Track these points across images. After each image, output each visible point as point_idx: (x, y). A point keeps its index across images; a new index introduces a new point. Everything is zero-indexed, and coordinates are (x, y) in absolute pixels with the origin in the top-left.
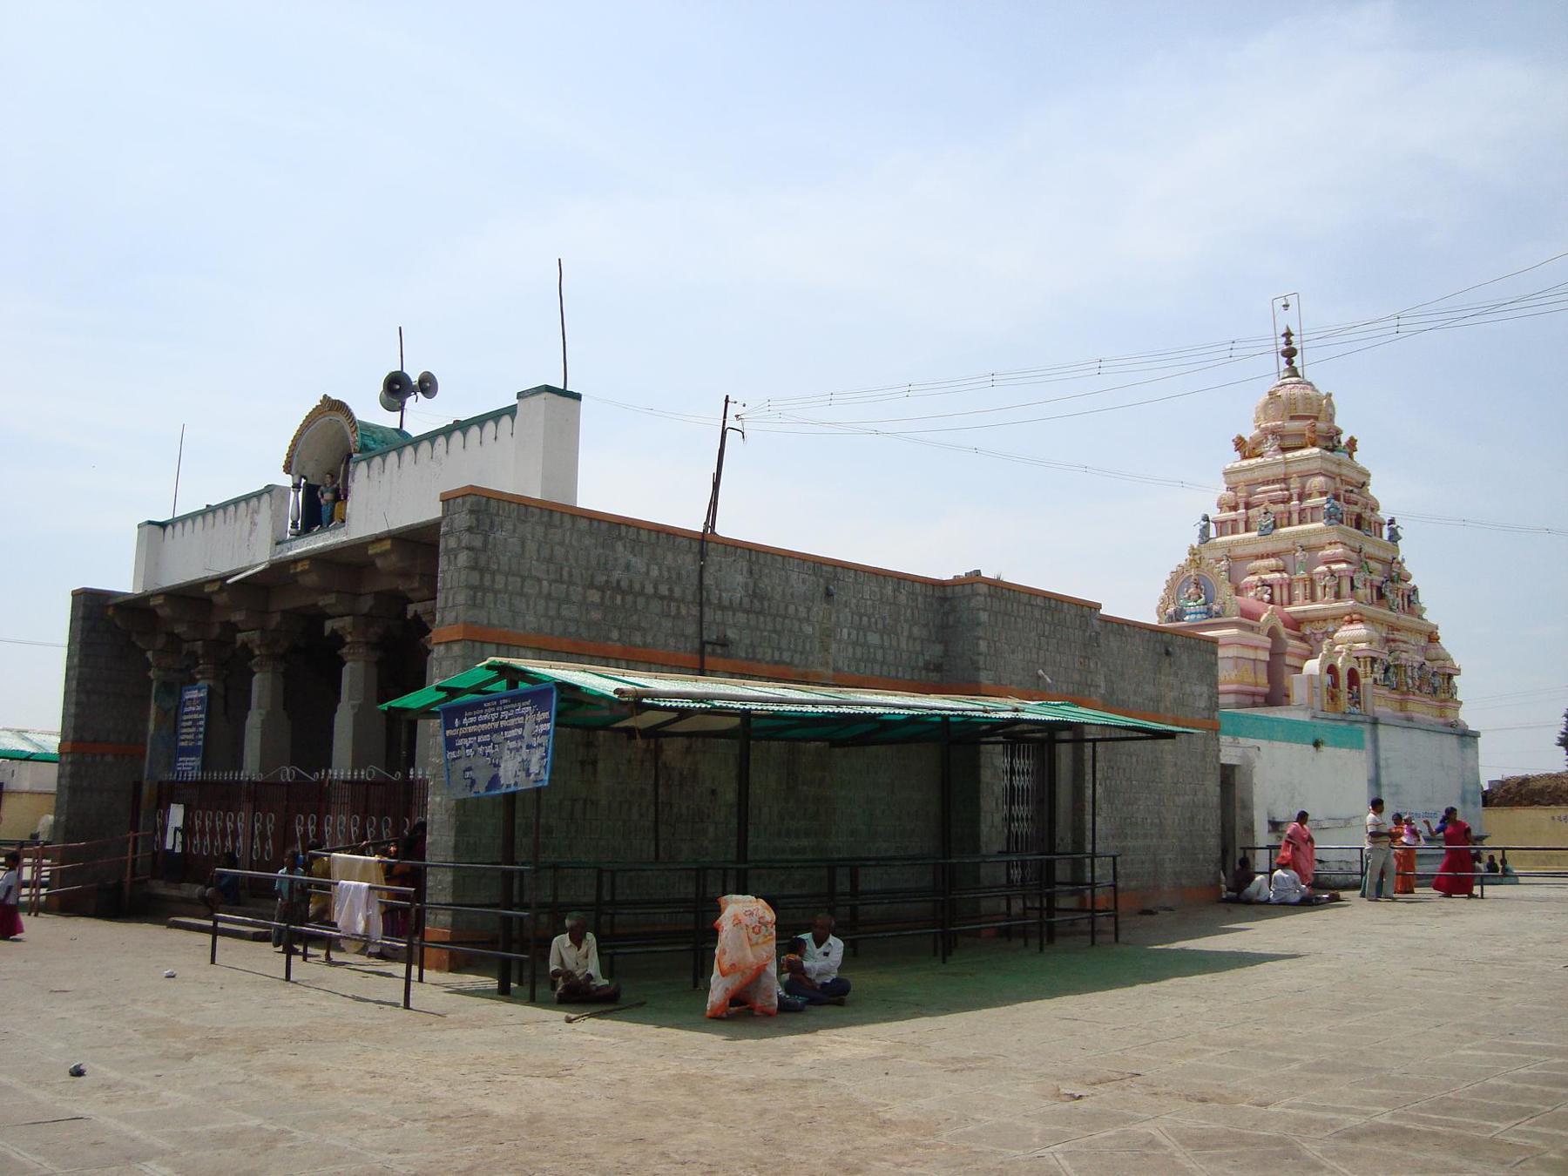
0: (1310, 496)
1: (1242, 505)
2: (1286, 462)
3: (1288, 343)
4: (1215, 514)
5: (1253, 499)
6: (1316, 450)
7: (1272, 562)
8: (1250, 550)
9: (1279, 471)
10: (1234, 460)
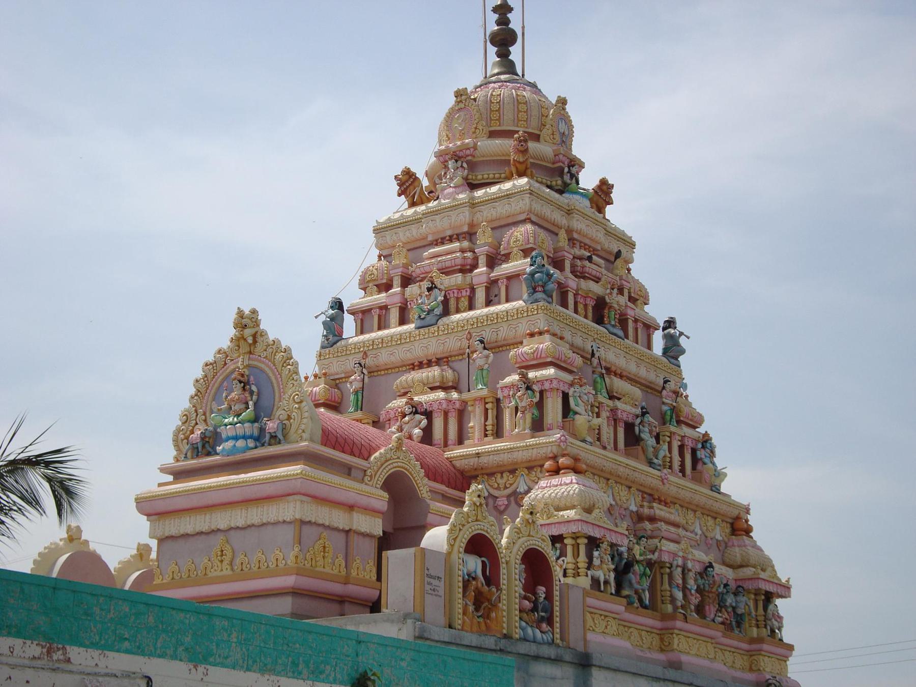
0: (507, 257)
1: (397, 281)
2: (473, 205)
3: (503, 21)
4: (353, 297)
5: (415, 270)
6: (524, 181)
7: (434, 373)
8: (401, 354)
9: (461, 220)
10: (395, 206)
